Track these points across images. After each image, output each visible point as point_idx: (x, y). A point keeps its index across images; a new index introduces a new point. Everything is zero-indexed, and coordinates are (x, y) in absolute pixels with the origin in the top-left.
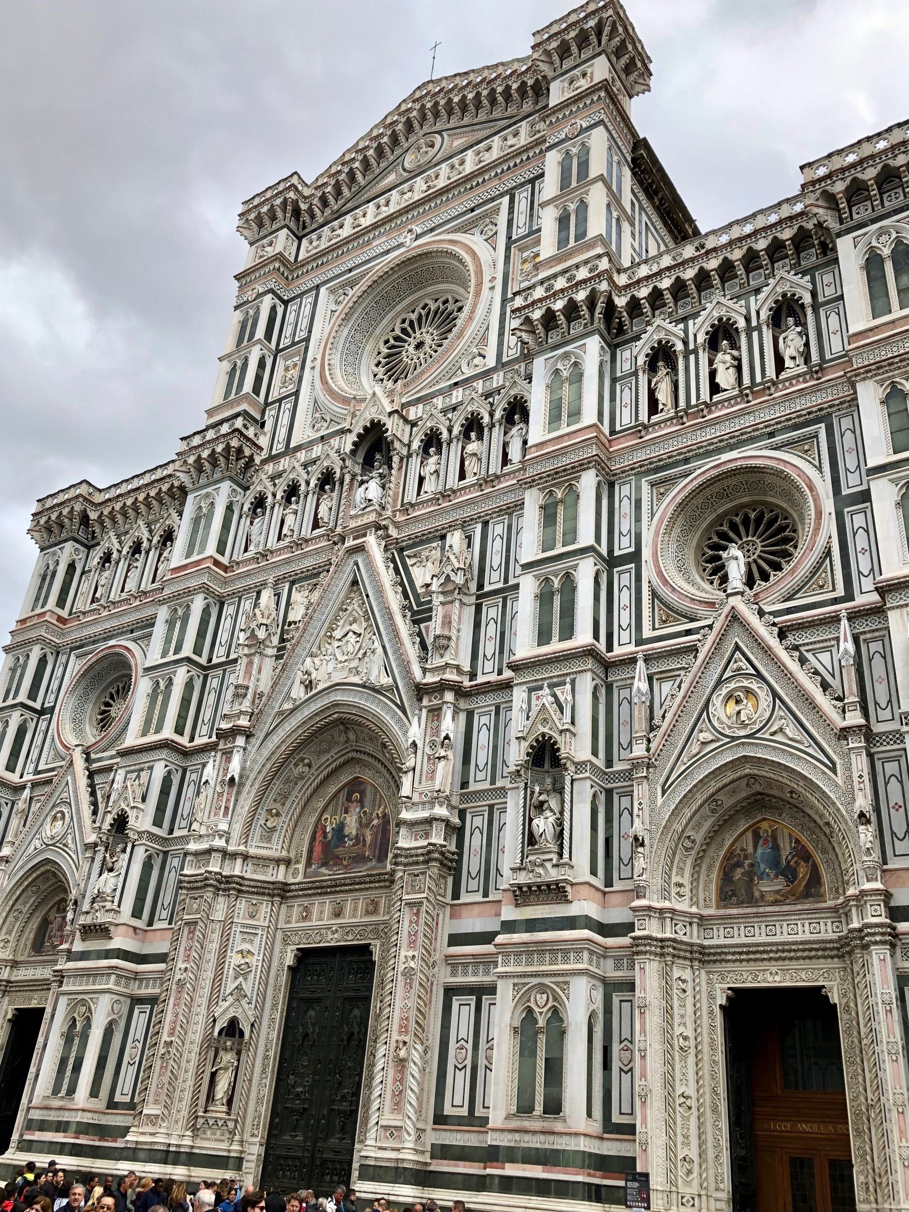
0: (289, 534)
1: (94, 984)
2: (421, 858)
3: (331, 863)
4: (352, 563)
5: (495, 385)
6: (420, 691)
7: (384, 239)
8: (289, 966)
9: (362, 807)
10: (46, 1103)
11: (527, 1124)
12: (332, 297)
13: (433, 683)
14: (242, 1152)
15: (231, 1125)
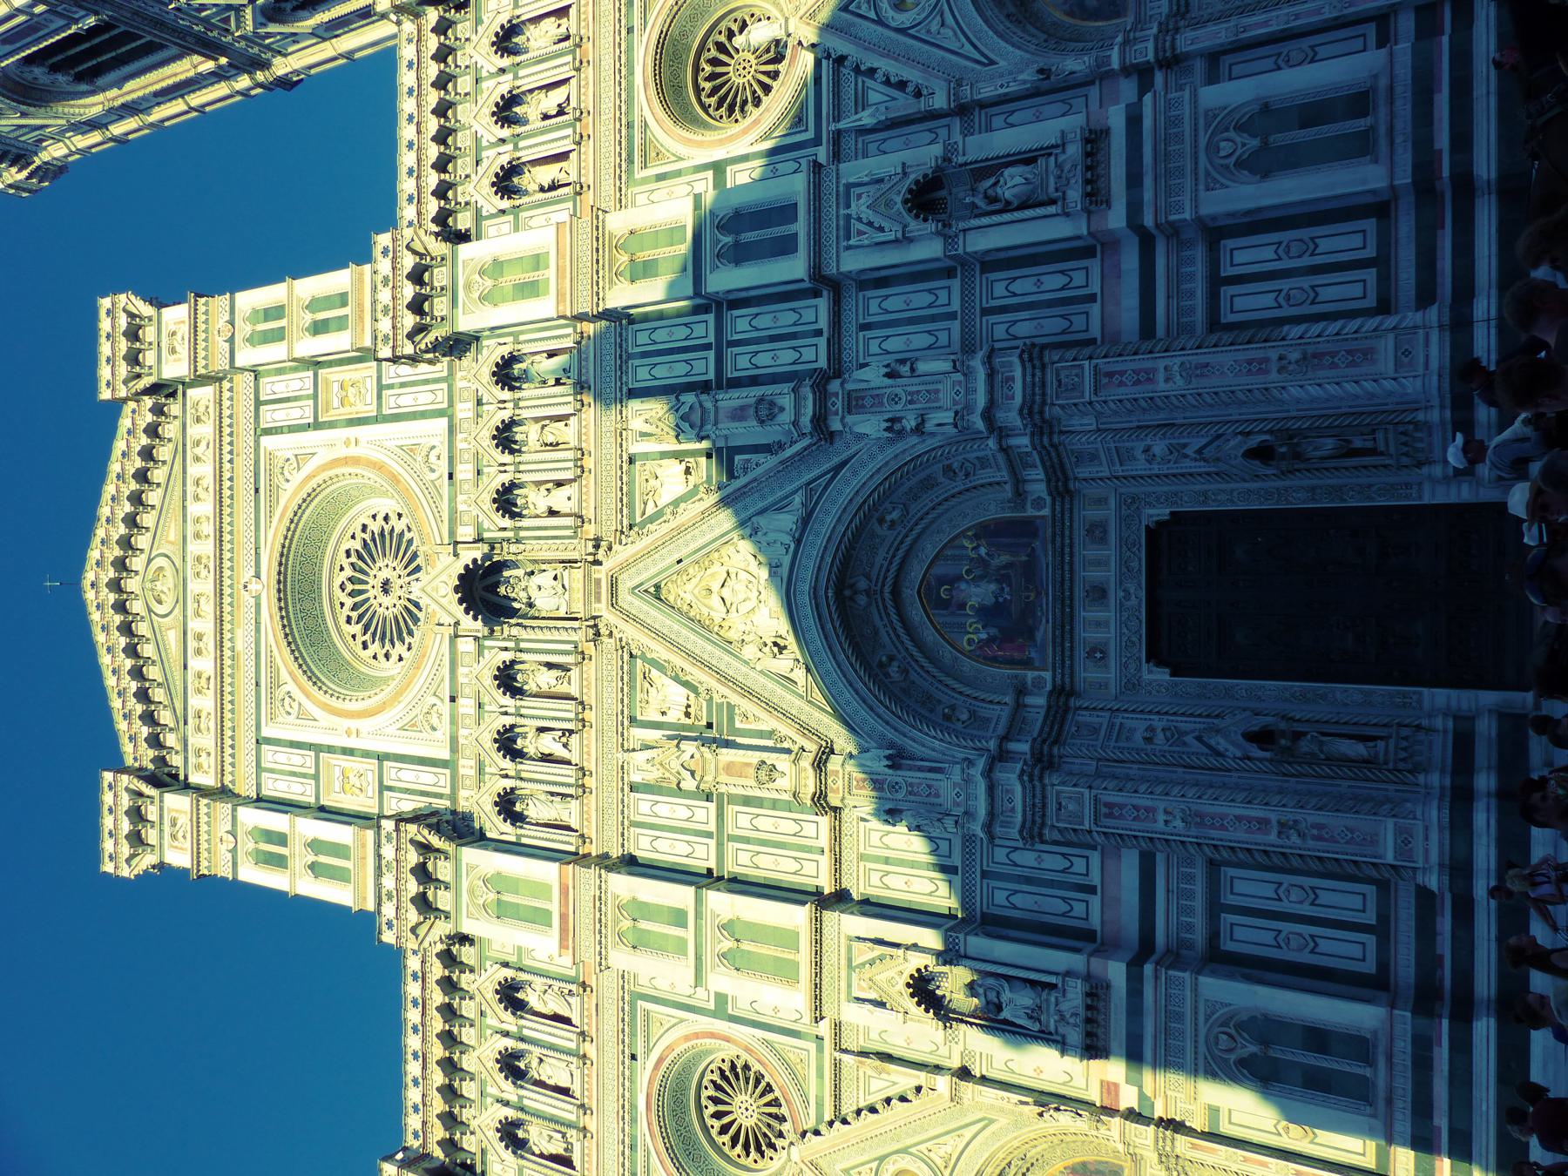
0: (564, 740)
1: (1180, 1017)
2: (1038, 373)
3: (1030, 622)
4: (630, 598)
5: (471, 414)
6: (820, 420)
7: (239, 633)
8: (1172, 675)
9: (960, 578)
10: (1381, 1104)
11: (1383, 129)
12: (280, 719)
13: (815, 405)
14: (1445, 715)
15: (1404, 732)
